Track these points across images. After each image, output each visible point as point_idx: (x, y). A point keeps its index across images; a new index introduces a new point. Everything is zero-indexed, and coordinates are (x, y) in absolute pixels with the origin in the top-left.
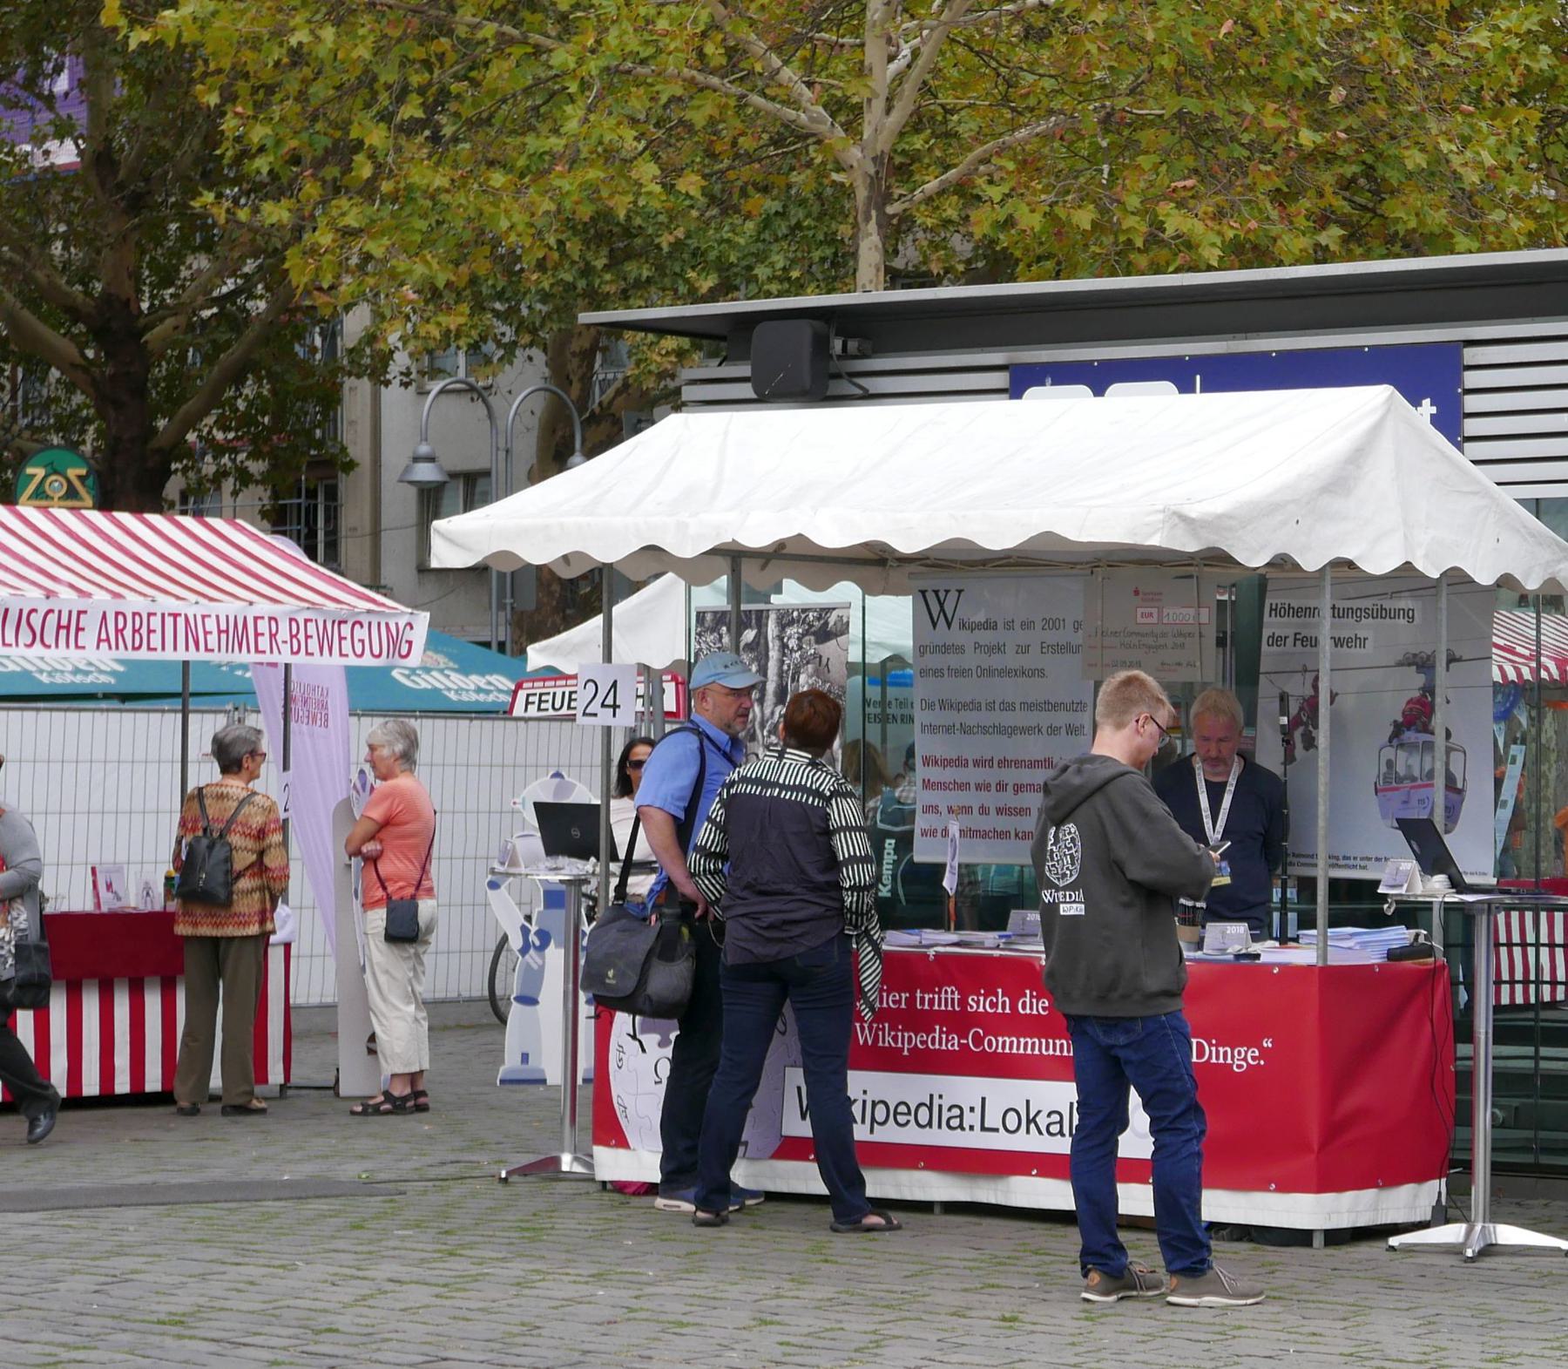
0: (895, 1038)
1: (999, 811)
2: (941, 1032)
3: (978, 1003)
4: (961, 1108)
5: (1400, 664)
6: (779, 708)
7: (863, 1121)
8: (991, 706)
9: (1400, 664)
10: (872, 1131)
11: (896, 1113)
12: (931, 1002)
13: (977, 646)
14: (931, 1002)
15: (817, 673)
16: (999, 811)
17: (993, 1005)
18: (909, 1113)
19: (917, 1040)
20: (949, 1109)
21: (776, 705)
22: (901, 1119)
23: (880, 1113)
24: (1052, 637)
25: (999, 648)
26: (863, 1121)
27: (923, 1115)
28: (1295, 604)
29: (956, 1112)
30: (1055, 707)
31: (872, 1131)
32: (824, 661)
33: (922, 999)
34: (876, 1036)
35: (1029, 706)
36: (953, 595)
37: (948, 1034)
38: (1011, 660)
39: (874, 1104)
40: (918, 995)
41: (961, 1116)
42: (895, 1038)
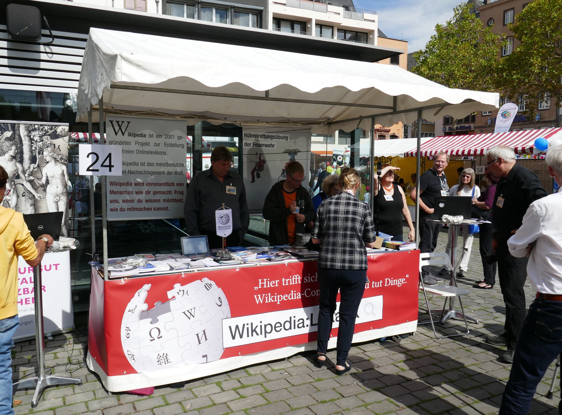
0: (274, 299)
1: (147, 201)
2: (294, 293)
3: (308, 279)
4: (303, 320)
5: (284, 153)
6: (33, 165)
7: (261, 334)
8: (143, 164)
9: (284, 153)
10: (266, 337)
11: (275, 327)
12: (289, 282)
13: (136, 142)
14: (289, 282)
15: (53, 151)
16: (147, 201)
17: (313, 279)
18: (281, 326)
19: (284, 298)
20: (298, 321)
21: (31, 164)
22: (278, 329)
23: (269, 329)
24: (169, 141)
25: (147, 144)
26: (261, 334)
27: (287, 325)
28: (252, 133)
29: (301, 321)
30: (170, 165)
31: (266, 337)
32: (57, 146)
33: (285, 282)
34: (265, 299)
35: (158, 164)
36: (125, 125)
37: (296, 293)
38: (151, 148)
39: (265, 326)
40: (283, 280)
41: (303, 323)
42: (274, 299)
